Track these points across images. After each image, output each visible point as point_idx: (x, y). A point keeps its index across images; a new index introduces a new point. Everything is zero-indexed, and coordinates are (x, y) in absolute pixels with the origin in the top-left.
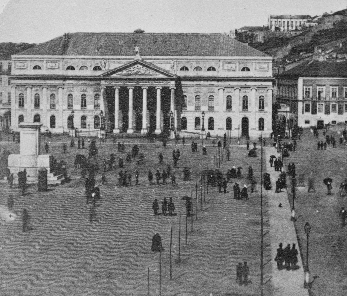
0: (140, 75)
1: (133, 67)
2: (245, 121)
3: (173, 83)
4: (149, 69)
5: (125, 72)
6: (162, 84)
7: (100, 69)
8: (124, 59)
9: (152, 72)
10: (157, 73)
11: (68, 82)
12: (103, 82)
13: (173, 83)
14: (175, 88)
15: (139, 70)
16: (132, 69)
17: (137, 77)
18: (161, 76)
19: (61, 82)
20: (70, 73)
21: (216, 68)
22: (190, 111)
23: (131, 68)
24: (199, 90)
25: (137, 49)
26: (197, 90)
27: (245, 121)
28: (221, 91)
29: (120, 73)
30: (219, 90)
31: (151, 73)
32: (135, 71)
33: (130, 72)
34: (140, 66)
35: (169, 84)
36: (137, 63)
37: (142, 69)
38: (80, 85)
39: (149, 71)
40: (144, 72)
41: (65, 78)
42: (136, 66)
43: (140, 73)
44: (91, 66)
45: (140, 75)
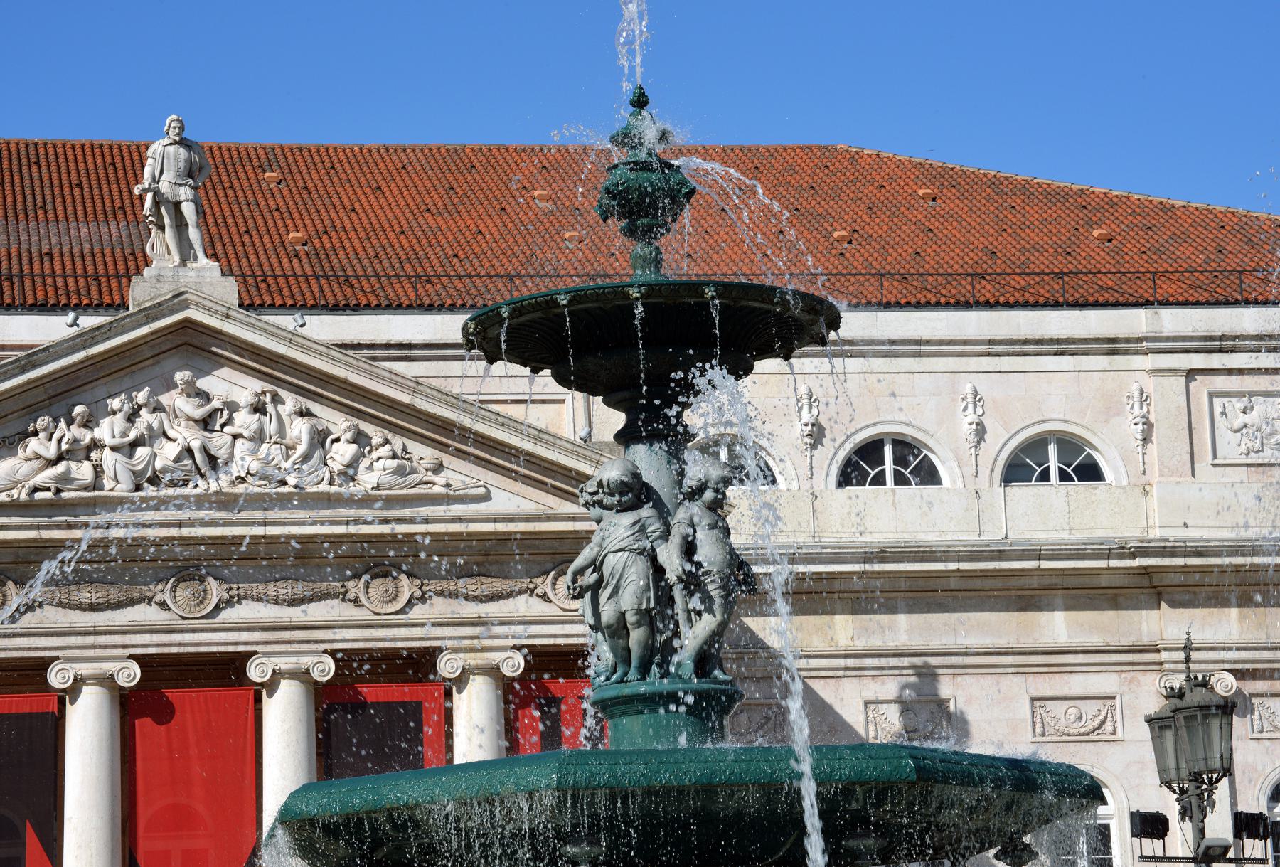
0: (225, 502)
4: (339, 423)
6: (523, 606)
10: (461, 474)
15: (218, 443)
17: (207, 526)
37: (244, 421)
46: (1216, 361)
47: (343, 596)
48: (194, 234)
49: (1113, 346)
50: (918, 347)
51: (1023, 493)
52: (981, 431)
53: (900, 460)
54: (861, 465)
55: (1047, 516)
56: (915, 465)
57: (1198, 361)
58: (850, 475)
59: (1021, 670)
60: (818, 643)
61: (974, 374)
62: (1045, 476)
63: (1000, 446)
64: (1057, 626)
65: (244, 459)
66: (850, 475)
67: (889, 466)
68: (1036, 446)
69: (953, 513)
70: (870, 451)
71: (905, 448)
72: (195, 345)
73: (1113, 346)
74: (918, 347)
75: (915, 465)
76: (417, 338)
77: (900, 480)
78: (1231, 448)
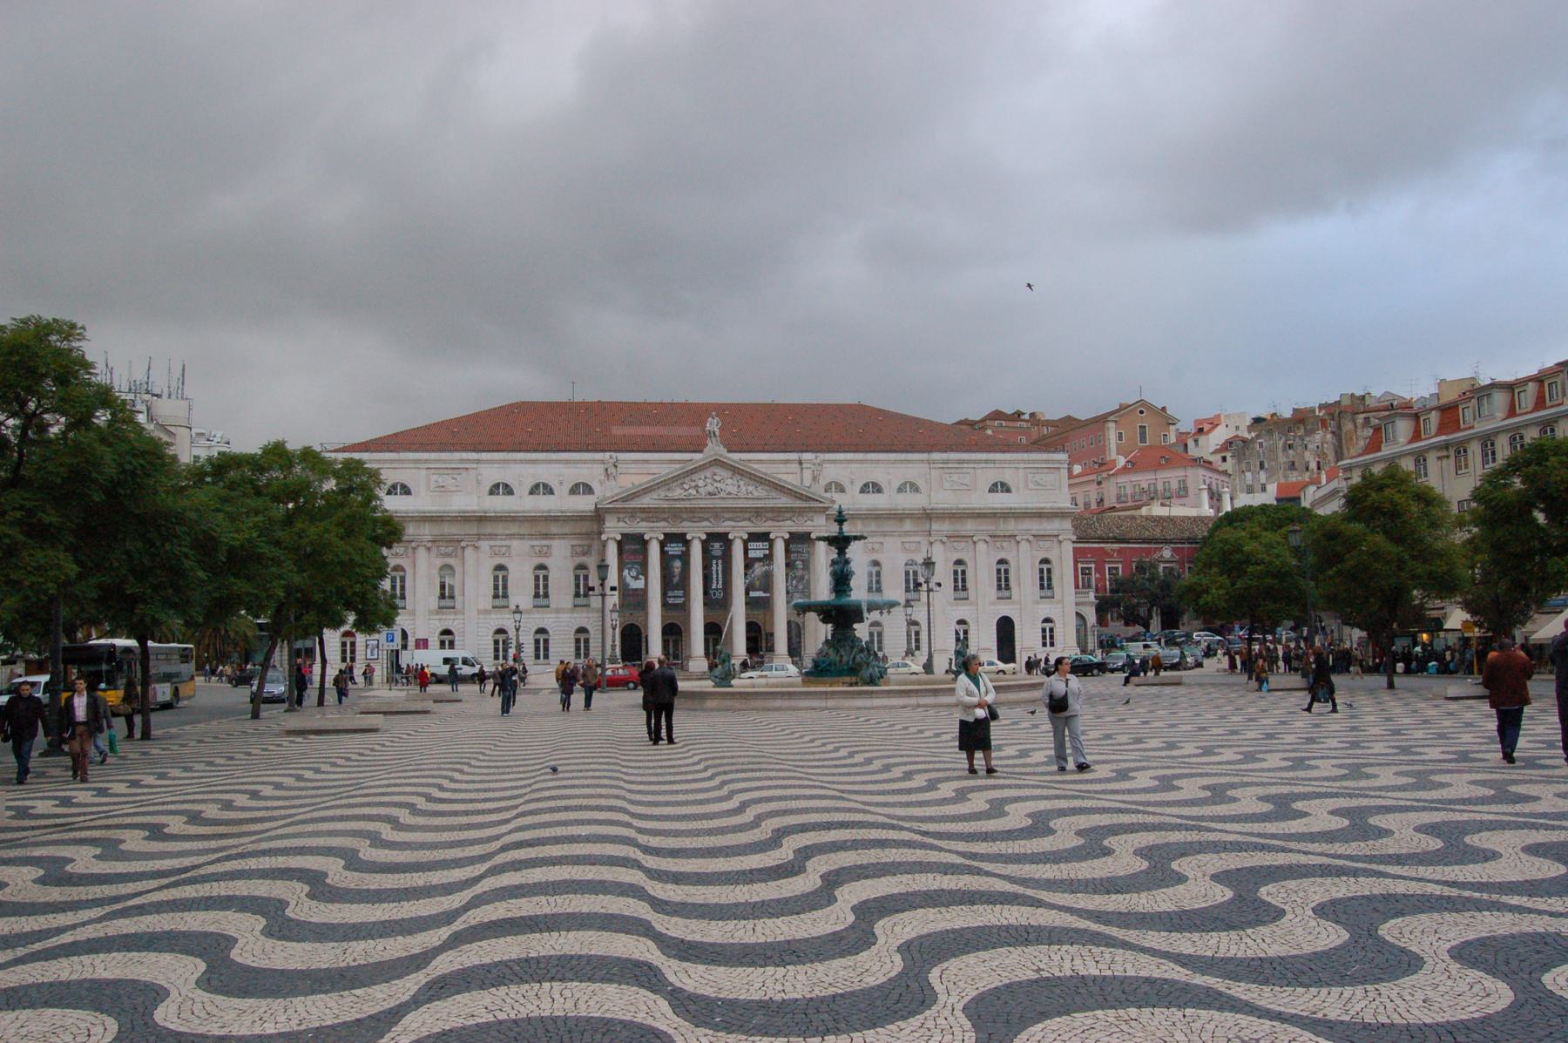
2: (1005, 629)
7: (588, 490)
9: (760, 492)
10: (774, 494)
11: (488, 528)
16: (701, 483)
18: (784, 501)
19: (472, 529)
20: (500, 504)
21: (920, 483)
24: (876, 546)
25: (713, 425)
27: (1005, 629)
31: (756, 494)
32: (710, 489)
34: (722, 473)
36: (717, 462)
38: (531, 536)
41: (482, 519)
43: (723, 495)
54: (865, 489)
55: (909, 502)
56: (877, 488)
58: (862, 491)
63: (897, 484)
64: (908, 525)
66: (862, 491)
70: (866, 485)
73: (922, 461)
74: (878, 461)
75: (877, 488)
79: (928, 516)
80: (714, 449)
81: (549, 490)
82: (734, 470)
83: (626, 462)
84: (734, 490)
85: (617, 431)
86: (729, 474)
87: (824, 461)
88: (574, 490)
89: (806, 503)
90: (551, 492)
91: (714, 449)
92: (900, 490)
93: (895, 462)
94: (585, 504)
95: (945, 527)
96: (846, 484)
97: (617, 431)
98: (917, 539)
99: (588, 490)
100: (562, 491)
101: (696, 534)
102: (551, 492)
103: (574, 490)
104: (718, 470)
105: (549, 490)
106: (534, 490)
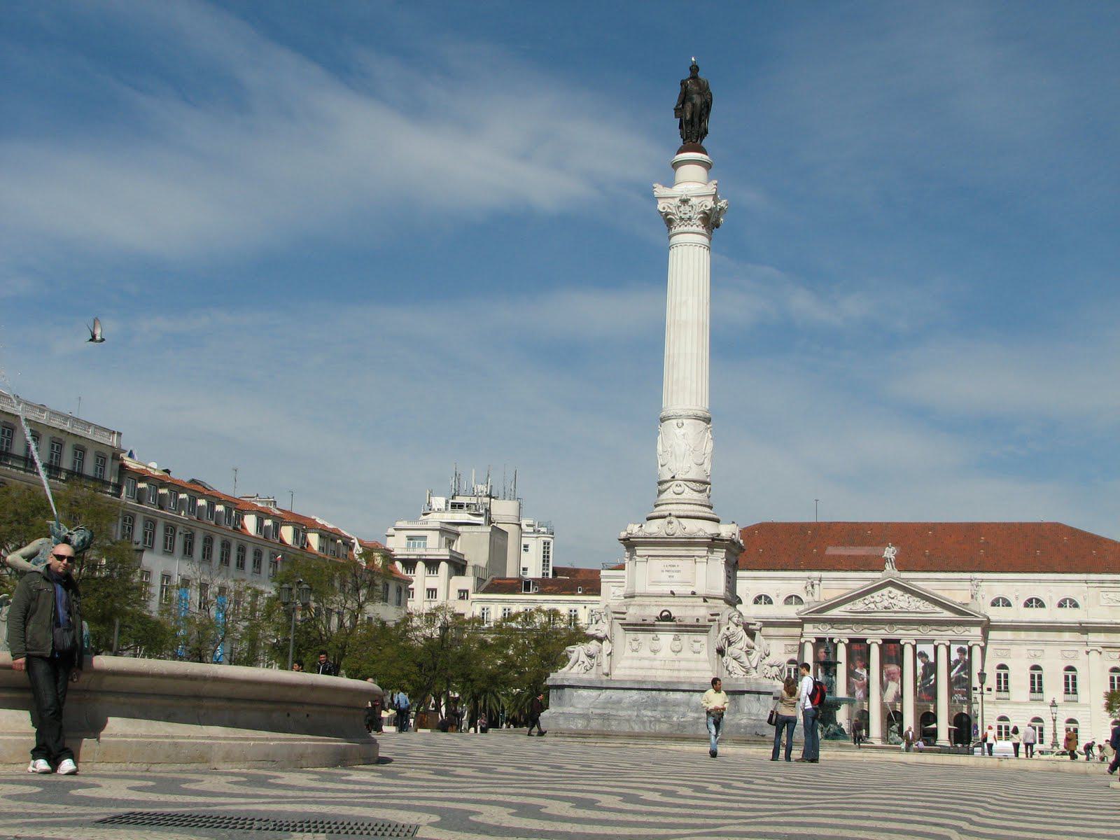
0: (895, 612)
1: (880, 593)
3: (977, 631)
5: (859, 605)
6: (950, 632)
7: (799, 600)
8: (855, 580)
10: (938, 609)
12: (808, 628)
13: (977, 631)
14: (982, 644)
16: (878, 599)
18: (947, 615)
21: (1079, 600)
22: (1018, 703)
23: (874, 594)
24: (1038, 653)
25: (890, 552)
26: (1032, 653)
28: (1094, 655)
29: (848, 607)
30: (1088, 653)
32: (886, 603)
33: (872, 606)
34: (895, 592)
35: (967, 633)
39: (918, 604)
40: (907, 605)
42: (885, 591)
43: (896, 609)
44: (778, 596)
45: (895, 612)
46: (1101, 585)
47: (917, 629)
48: (894, 564)
49: (1080, 581)
50: (1040, 581)
51: (1063, 609)
52: (1051, 598)
53: (1037, 603)
54: (1028, 603)
56: (1040, 604)
57: (1098, 585)
58: (1026, 605)
59: (1059, 645)
60: (1018, 638)
61: (1052, 586)
62: (1066, 607)
64: (1067, 636)
65: (902, 604)
66: (1026, 605)
67: (1034, 604)
68: (1064, 601)
69: (1049, 614)
70: (1030, 600)
71: (1038, 600)
72: (891, 584)
73: (1080, 581)
74: (1040, 581)
75: (1040, 604)
76: (941, 578)
77: (1036, 607)
78: (1103, 602)
79: (1084, 629)
80: (890, 572)
81: (769, 601)
82: (906, 590)
83: (828, 579)
84: (904, 605)
85: (831, 551)
86: (899, 593)
87: (982, 580)
88: (788, 600)
89: (963, 617)
90: (770, 602)
91: (890, 572)
92: (1060, 605)
93: (1055, 581)
94: (792, 612)
95: (1102, 638)
96: (1012, 600)
97: (831, 551)
98: (1076, 648)
99: (799, 600)
100: (778, 602)
101: (874, 637)
102: (770, 602)
103: (788, 600)
104: (890, 589)
105: (769, 601)
106: (757, 600)
